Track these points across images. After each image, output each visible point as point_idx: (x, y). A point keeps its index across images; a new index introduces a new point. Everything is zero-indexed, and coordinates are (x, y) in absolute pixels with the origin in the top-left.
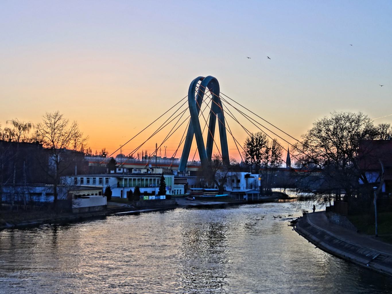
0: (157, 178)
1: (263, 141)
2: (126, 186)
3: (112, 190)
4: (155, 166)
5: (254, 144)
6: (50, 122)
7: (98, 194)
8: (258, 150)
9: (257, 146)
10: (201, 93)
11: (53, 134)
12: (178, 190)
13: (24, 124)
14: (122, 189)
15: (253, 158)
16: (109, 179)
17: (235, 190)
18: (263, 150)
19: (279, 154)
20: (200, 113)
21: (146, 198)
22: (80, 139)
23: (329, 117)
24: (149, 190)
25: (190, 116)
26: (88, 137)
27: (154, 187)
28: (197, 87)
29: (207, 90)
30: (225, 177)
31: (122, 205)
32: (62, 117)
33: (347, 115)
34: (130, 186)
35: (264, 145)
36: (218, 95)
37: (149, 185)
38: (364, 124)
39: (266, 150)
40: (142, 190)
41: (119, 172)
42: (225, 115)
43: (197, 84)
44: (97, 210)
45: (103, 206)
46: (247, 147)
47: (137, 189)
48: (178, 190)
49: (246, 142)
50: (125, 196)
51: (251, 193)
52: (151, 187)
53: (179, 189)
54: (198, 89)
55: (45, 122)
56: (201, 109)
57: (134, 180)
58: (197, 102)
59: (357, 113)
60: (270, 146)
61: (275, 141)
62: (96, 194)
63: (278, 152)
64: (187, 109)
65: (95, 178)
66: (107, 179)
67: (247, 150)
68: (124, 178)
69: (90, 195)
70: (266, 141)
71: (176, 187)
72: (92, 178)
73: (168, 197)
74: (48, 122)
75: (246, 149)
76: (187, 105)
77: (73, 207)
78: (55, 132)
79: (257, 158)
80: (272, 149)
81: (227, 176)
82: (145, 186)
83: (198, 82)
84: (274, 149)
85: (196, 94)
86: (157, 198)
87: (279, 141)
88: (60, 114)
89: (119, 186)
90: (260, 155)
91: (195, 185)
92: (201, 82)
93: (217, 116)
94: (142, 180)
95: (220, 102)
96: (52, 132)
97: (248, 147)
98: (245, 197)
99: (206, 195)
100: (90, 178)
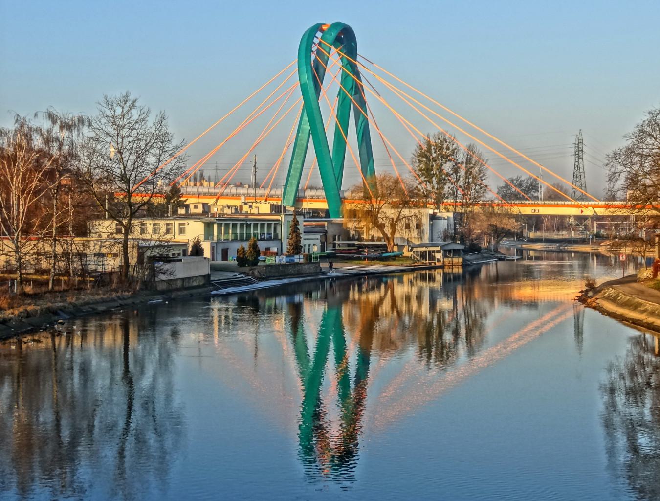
5: (431, 154)
6: (113, 112)
12: (309, 245)
13: (71, 116)
15: (430, 182)
16: (186, 224)
18: (447, 167)
19: (479, 174)
22: (169, 147)
26: (184, 142)
27: (270, 239)
28: (315, 43)
30: (398, 219)
31: (230, 275)
32: (137, 104)
36: (355, 60)
39: (454, 166)
40: (262, 245)
44: (195, 284)
45: (205, 276)
46: (419, 160)
48: (309, 245)
49: (416, 151)
53: (312, 242)
55: (103, 113)
60: (461, 157)
63: (477, 169)
66: (168, 225)
67: (419, 166)
70: (455, 149)
71: (307, 239)
72: (151, 222)
74: (109, 113)
75: (417, 165)
77: (157, 279)
79: (439, 183)
80: (466, 163)
81: (401, 217)
83: (316, 35)
86: (288, 259)
88: (132, 98)
91: (339, 236)
97: (420, 162)
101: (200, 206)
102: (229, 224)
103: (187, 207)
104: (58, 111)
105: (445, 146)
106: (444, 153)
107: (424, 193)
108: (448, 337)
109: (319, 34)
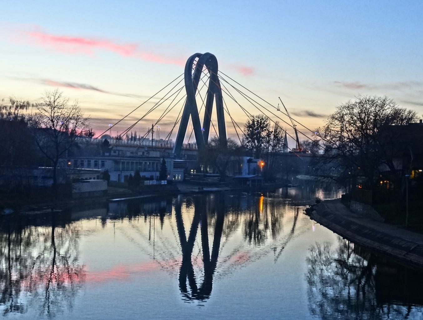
0: (156, 162)
1: (264, 124)
2: (123, 170)
3: (110, 174)
4: (151, 149)
5: (255, 126)
7: (96, 178)
8: (259, 133)
9: (257, 129)
10: (199, 71)
11: (53, 113)
13: (23, 101)
14: (119, 173)
15: (254, 142)
18: (264, 134)
19: (281, 138)
20: (197, 92)
21: (147, 183)
23: (353, 101)
24: (147, 174)
25: (186, 96)
27: (153, 171)
28: (194, 64)
29: (204, 67)
33: (372, 98)
34: (128, 170)
35: (265, 129)
37: (147, 169)
38: (389, 108)
41: (114, 154)
42: (224, 94)
43: (194, 61)
46: (248, 130)
47: (137, 173)
50: (123, 181)
52: (150, 171)
54: (195, 66)
56: (198, 88)
57: (132, 163)
58: (193, 81)
59: (383, 97)
61: (277, 124)
62: (94, 179)
64: (183, 87)
65: (90, 161)
67: (248, 132)
68: (122, 161)
69: (88, 178)
70: (268, 124)
72: (86, 160)
73: (170, 182)
75: (247, 132)
76: (183, 83)
77: (73, 192)
78: (55, 112)
82: (143, 170)
83: (195, 59)
84: (277, 132)
85: (193, 72)
87: (282, 124)
89: (117, 170)
90: (261, 139)
92: (199, 59)
93: (215, 95)
95: (219, 81)
96: (52, 111)
97: (248, 130)
98: (248, 183)
99: (208, 181)
100: (84, 161)
101: (117, 152)
102: (129, 162)
103: (110, 152)
105: (262, 122)
106: (262, 126)
107: (250, 147)
108: (261, 227)
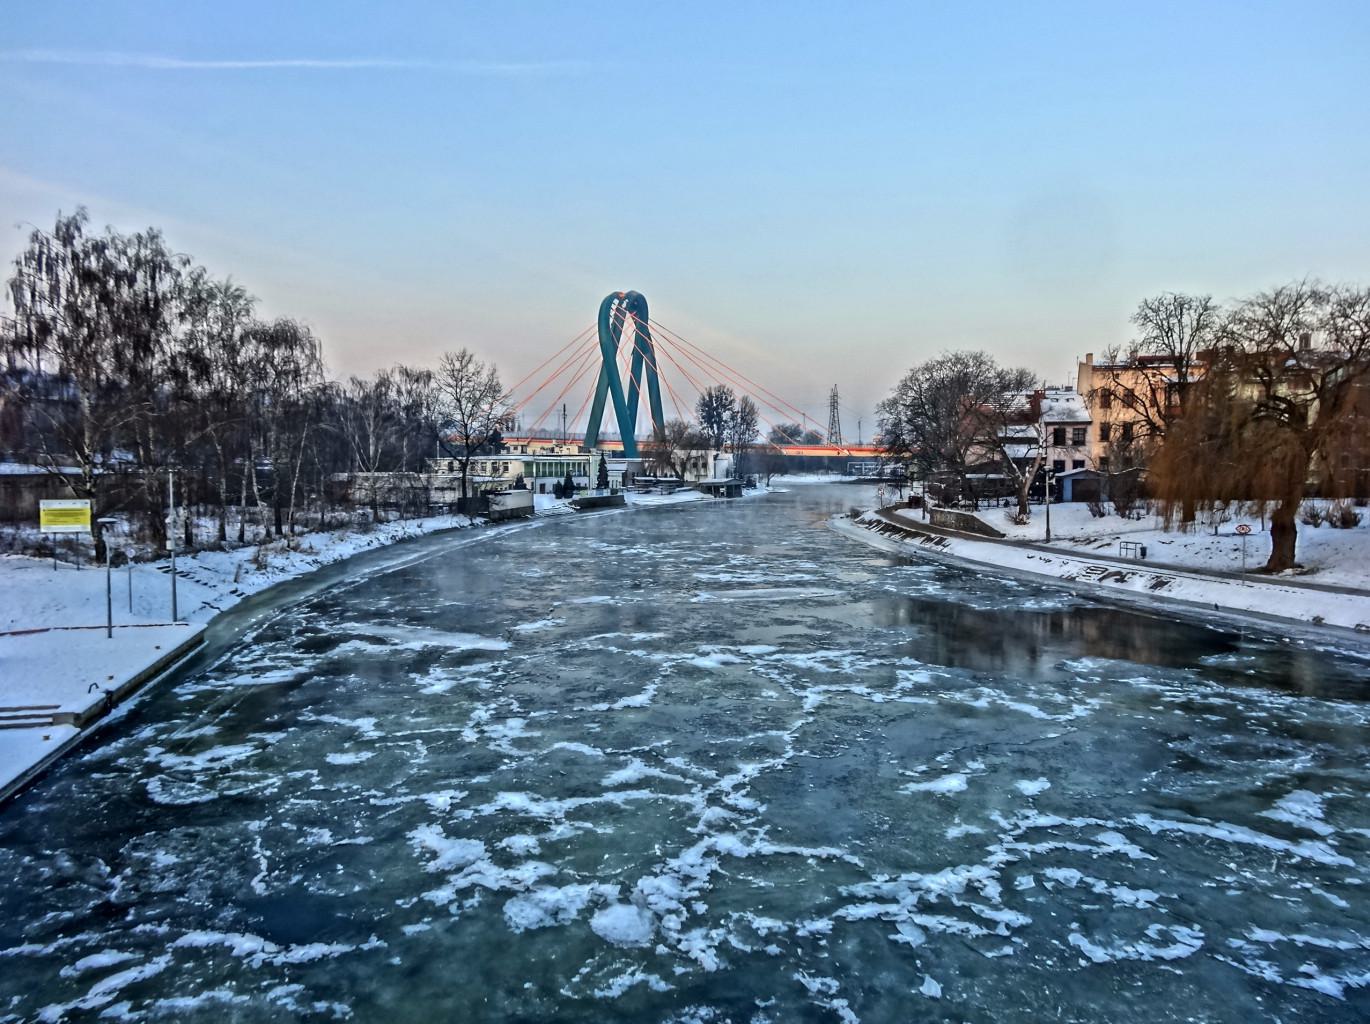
8: (719, 415)
15: (712, 428)
17: (702, 480)
32: (474, 359)
34: (544, 475)
42: (658, 355)
51: (733, 483)
60: (737, 407)
61: (745, 400)
74: (448, 367)
87: (752, 399)
88: (468, 353)
94: (562, 464)
95: (649, 335)
98: (722, 490)
104: (409, 365)
109: (616, 301)
